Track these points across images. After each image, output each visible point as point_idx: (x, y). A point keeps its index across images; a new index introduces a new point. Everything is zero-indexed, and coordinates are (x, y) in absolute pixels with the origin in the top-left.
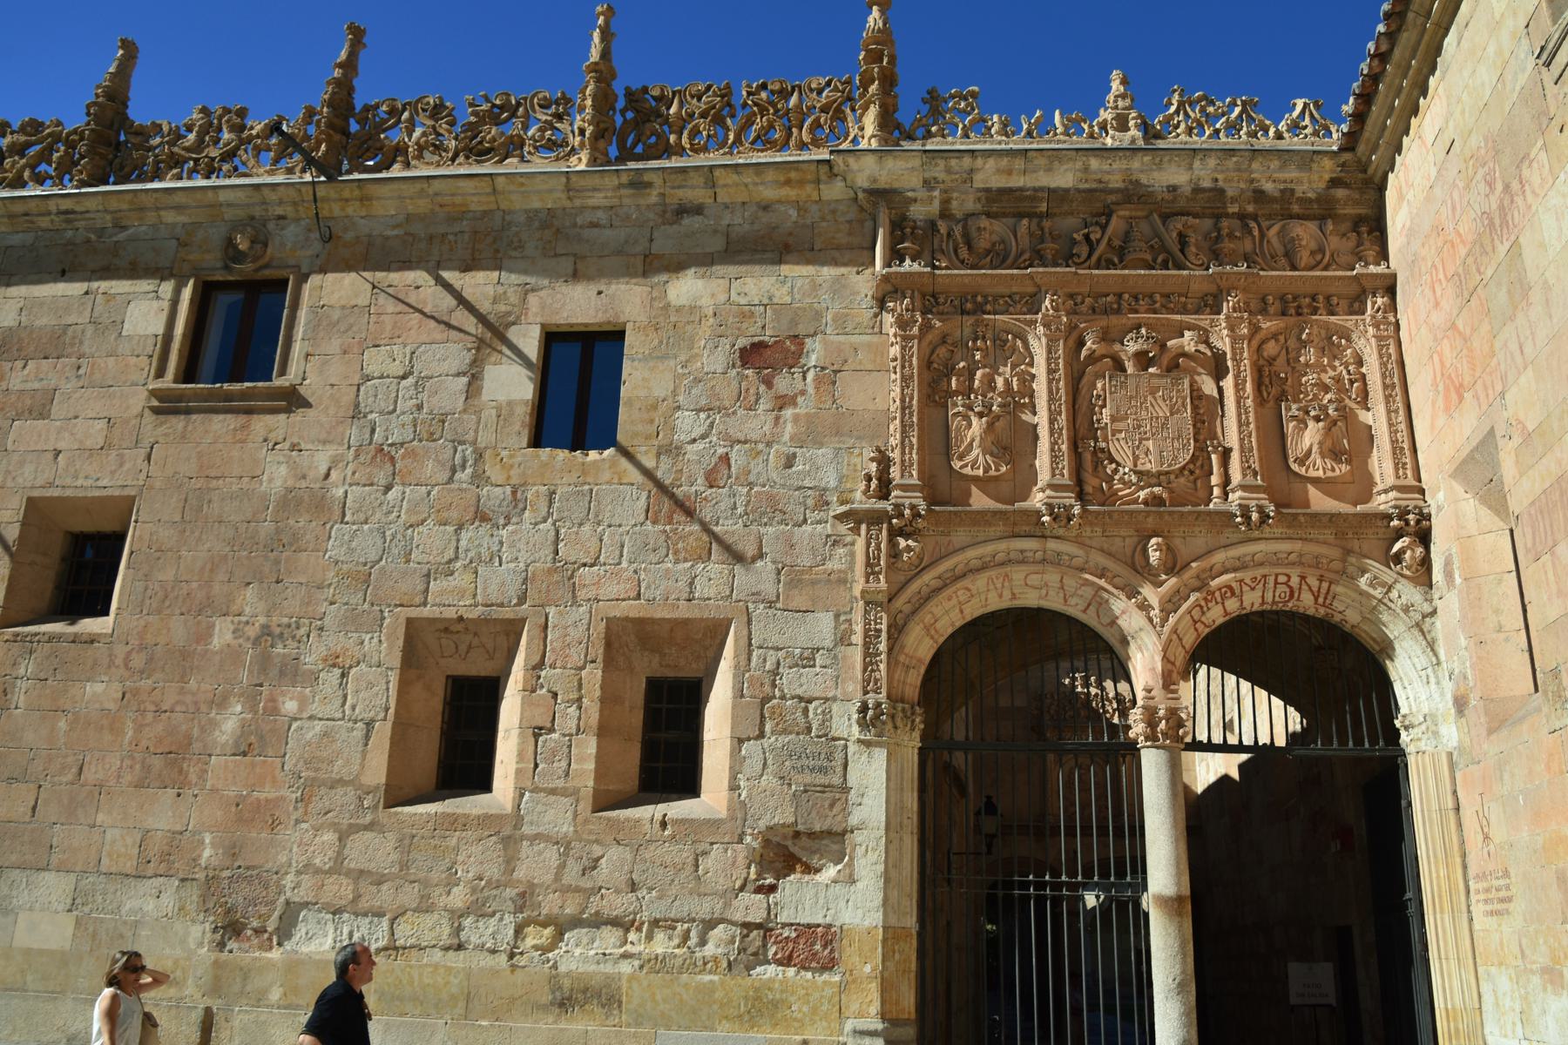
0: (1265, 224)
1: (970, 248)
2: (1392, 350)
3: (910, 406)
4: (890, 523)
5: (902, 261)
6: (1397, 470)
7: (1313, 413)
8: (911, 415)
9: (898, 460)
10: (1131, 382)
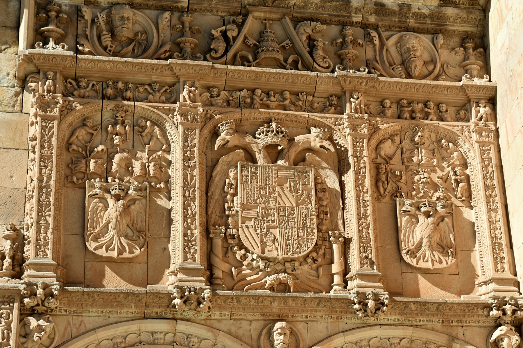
0: (384, 34)
1: (113, 36)
3: (48, 186)
4: (22, 302)
5: (46, 43)
6: (496, 263)
7: (423, 209)
8: (48, 194)
9: (33, 239)
10: (262, 174)
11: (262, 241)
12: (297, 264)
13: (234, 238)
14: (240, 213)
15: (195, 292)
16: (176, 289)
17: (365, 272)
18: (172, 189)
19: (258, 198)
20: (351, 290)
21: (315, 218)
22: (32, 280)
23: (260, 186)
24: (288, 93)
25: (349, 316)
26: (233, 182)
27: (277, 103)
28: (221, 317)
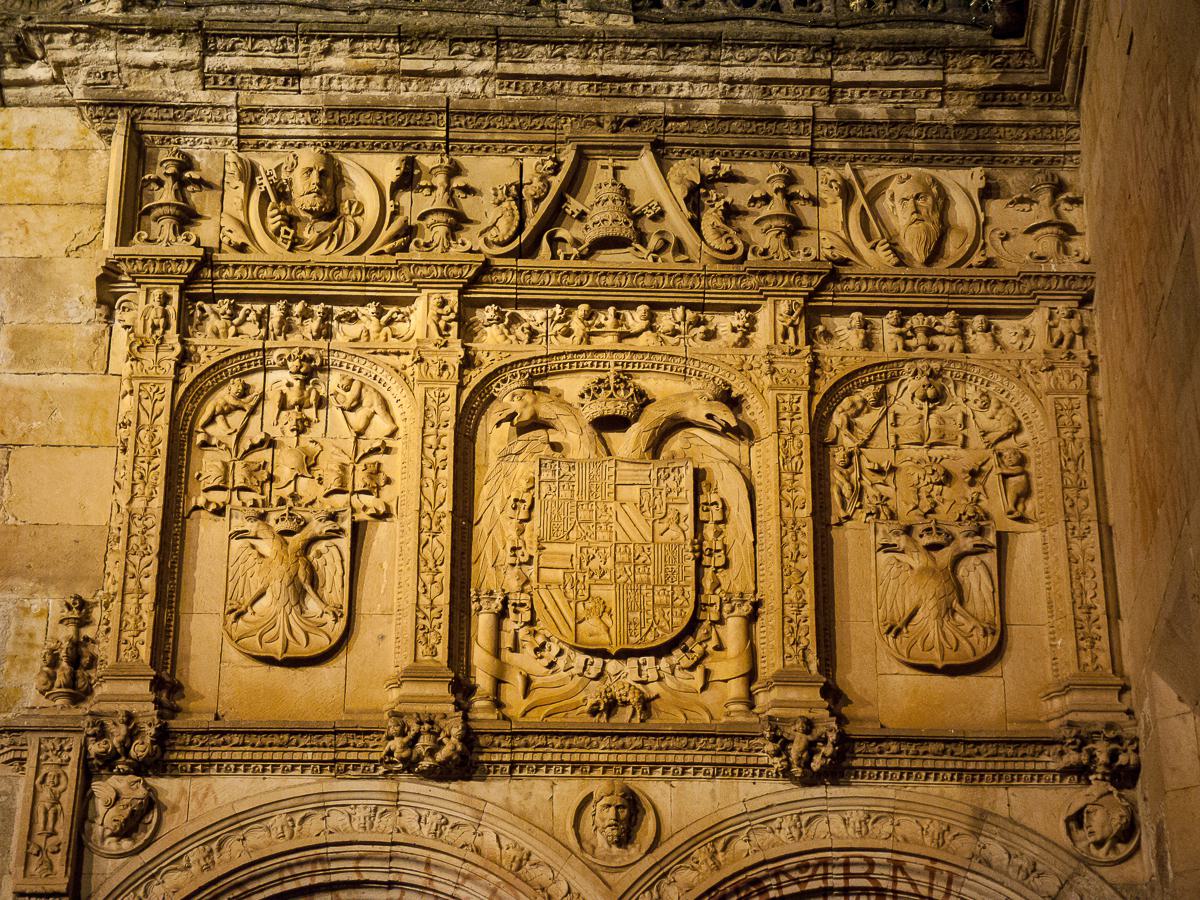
2: (1081, 418)
22: (105, 707)
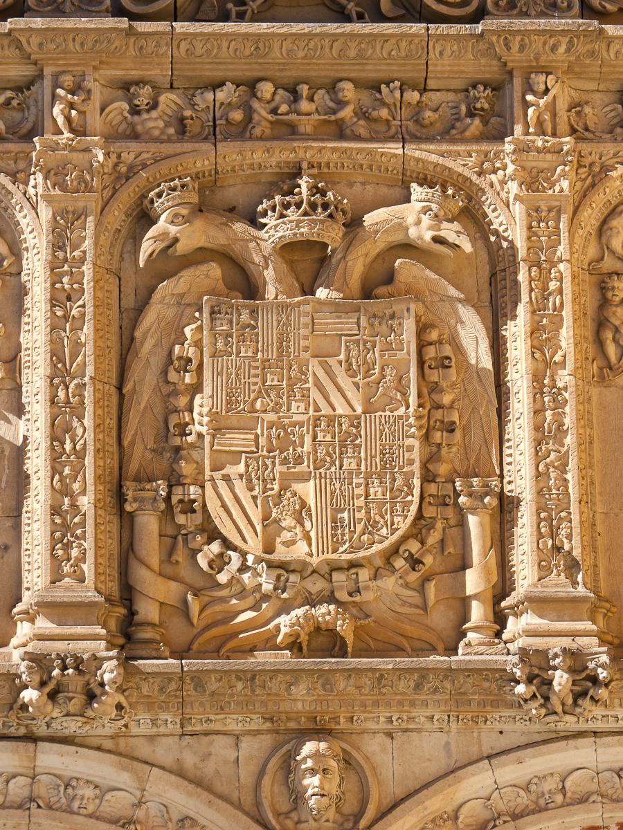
10: (268, 325)
11: (266, 517)
12: (364, 574)
13: (194, 511)
14: (207, 439)
15: (77, 668)
16: (26, 662)
17: (551, 591)
18: (24, 381)
19: (259, 395)
20: (512, 641)
21: (416, 443)
23: (264, 361)
24: (348, 86)
25: (507, 713)
26: (191, 352)
27: (316, 117)
28: (155, 729)
